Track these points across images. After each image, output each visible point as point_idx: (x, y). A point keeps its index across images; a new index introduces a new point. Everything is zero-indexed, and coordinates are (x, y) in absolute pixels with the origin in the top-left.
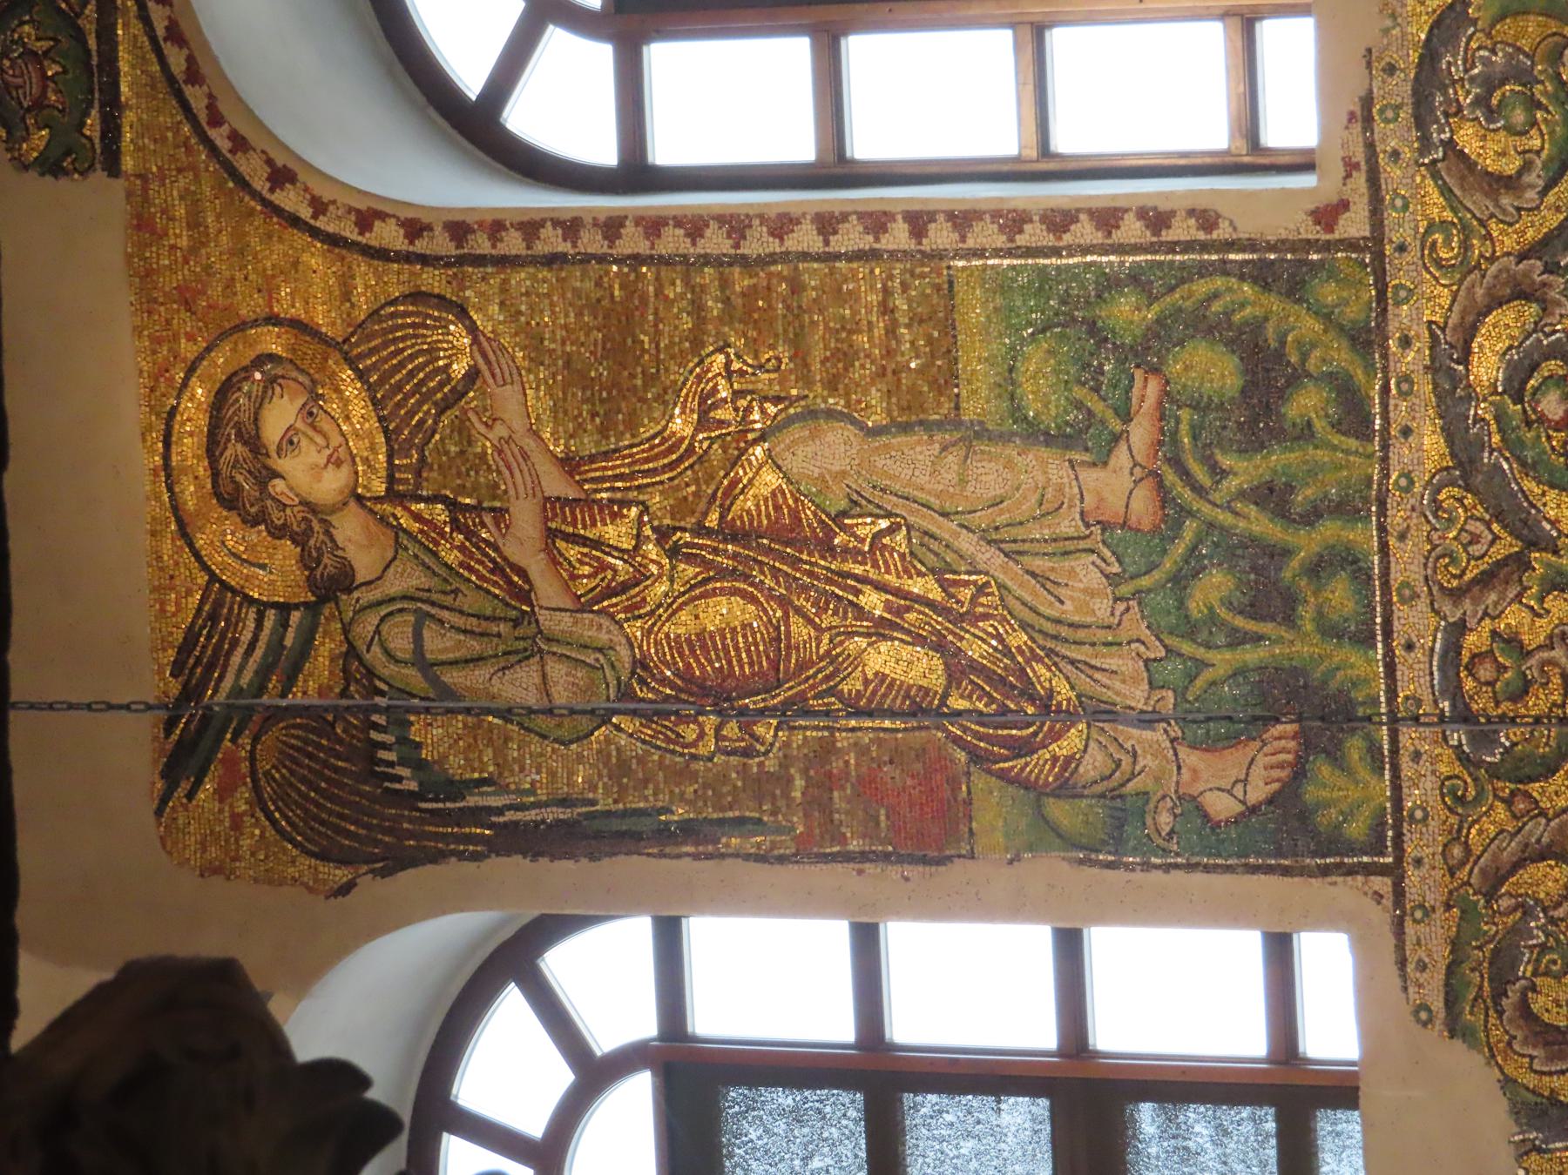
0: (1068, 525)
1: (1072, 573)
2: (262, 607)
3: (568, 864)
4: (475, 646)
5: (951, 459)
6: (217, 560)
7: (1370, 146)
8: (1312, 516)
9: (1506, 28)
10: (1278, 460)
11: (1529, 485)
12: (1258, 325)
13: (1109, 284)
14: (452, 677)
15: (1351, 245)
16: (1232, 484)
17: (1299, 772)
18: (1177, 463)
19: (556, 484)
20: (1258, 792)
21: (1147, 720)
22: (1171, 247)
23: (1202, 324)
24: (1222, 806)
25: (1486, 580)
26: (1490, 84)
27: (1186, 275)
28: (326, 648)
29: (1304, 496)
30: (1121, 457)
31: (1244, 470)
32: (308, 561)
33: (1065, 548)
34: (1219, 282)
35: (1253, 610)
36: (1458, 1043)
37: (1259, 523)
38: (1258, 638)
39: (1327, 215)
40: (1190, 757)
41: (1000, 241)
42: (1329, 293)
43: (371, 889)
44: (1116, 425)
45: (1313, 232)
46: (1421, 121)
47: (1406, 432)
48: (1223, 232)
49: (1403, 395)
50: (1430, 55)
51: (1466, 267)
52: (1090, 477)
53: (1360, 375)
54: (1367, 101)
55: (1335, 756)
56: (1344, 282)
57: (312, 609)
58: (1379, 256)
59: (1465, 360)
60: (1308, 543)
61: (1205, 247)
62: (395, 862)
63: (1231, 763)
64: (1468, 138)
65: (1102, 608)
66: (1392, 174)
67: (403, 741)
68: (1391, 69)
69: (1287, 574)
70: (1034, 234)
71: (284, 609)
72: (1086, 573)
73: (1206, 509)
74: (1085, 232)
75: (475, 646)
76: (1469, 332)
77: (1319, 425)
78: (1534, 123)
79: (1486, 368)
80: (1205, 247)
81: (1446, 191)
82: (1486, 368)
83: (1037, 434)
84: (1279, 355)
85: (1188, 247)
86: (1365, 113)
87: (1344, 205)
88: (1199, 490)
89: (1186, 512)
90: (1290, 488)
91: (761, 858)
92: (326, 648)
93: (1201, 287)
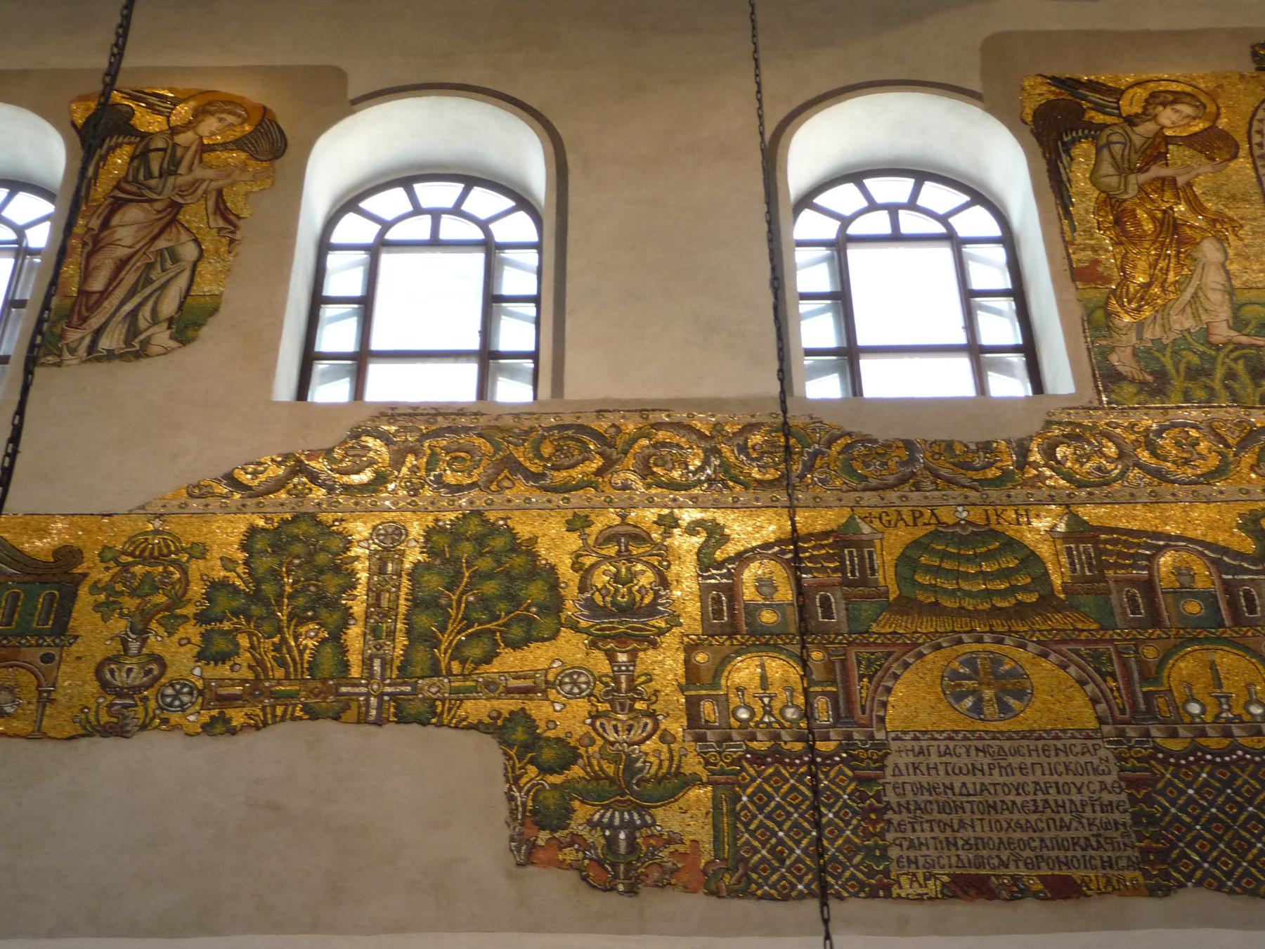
0: (1205, 318)
1: (1187, 319)
2: (1117, 103)
3: (1048, 180)
4: (1118, 158)
5: (1220, 287)
6: (1131, 91)
10: (1245, 377)
14: (1105, 152)
17: (1132, 381)
19: (1181, 181)
20: (1121, 369)
21: (1140, 338)
24: (1114, 358)
25: (1218, 435)
28: (1109, 120)
30: (1233, 333)
31: (1240, 367)
32: (1136, 115)
33: (1196, 316)
35: (1188, 368)
36: (1042, 424)
37: (1220, 372)
38: (1177, 371)
40: (1129, 350)
43: (1026, 131)
52: (1224, 324)
55: (1140, 392)
57: (1120, 116)
60: (1217, 385)
62: (1038, 135)
63: (1130, 361)
65: (1177, 327)
67: (1080, 138)
69: (1204, 379)
71: (1118, 108)
72: (1189, 323)
75: (1118, 158)
83: (1236, 309)
88: (1227, 356)
91: (1062, 233)
92: (1109, 120)
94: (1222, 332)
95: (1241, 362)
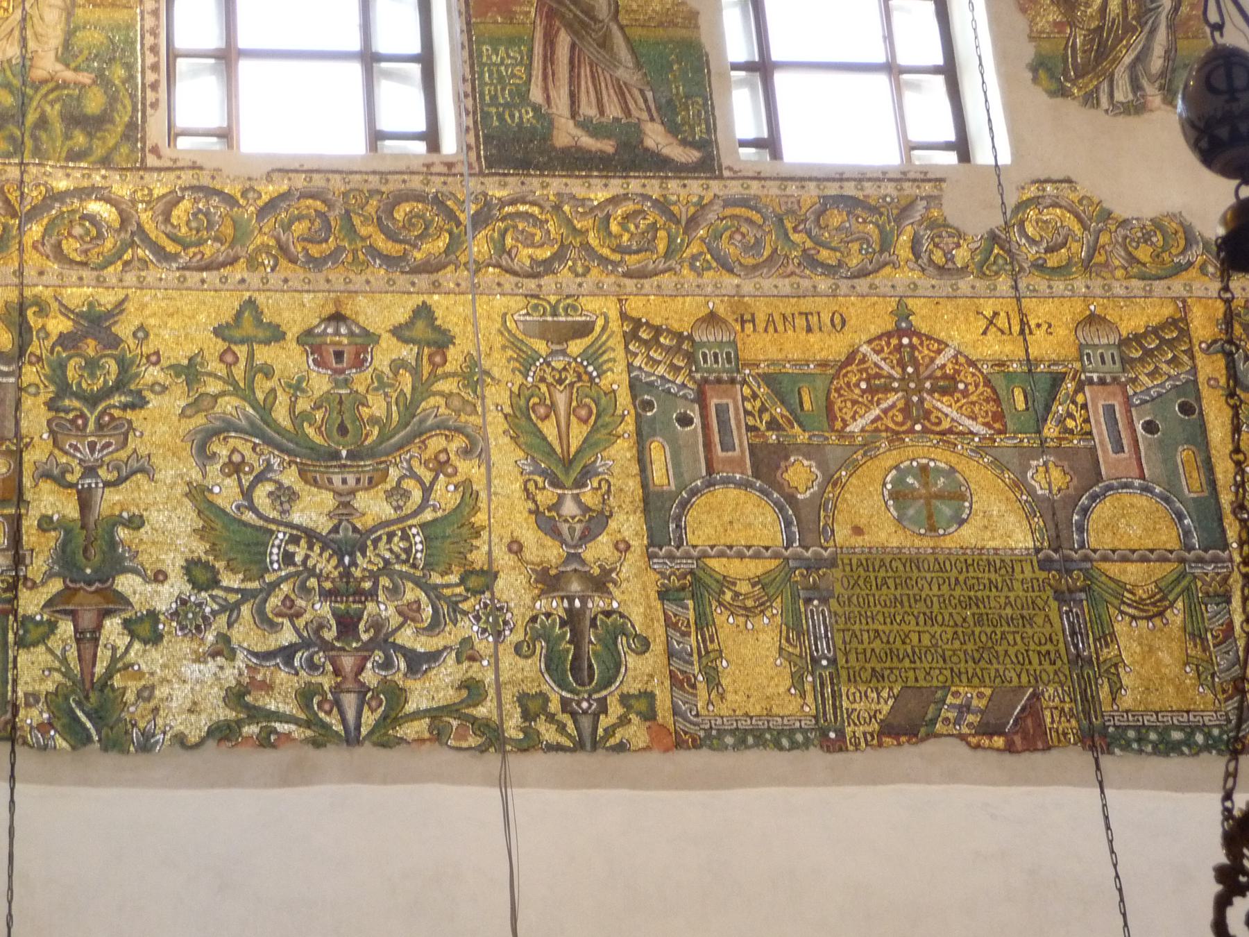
1: (12, 45)
7: (182, 168)
8: (35, 138)
9: (228, 222)
10: (58, 127)
11: (45, 221)
12: (112, 121)
13: (129, 67)
15: (143, 160)
16: (48, 109)
18: (57, 87)
22: (144, 91)
23: (113, 100)
26: (207, 214)
27: (132, 97)
29: (44, 136)
30: (59, 67)
31: (53, 112)
34: (129, 108)
37: (31, 118)
39: (155, 151)
41: (147, 27)
42: (124, 150)
44: (73, 65)
45: (149, 144)
46: (193, 188)
47: (68, 175)
48: (148, 109)
49: (83, 176)
50: (219, 193)
51: (134, 202)
52: (52, 55)
53: (92, 159)
54: (201, 168)
56: (128, 156)
58: (139, 169)
59: (96, 199)
61: (144, 104)
64: (185, 204)
66: (172, 176)
68: (213, 178)
70: (149, 40)
73: (38, 97)
74: (150, 59)
76: (108, 200)
77: (69, 143)
78: (191, 229)
79: (94, 207)
80: (144, 104)
81: (164, 196)
82: (94, 207)
83: (70, 34)
84: (99, 129)
85: (144, 98)
86: (195, 167)
87: (159, 157)
88: (46, 95)
89: (37, 90)
90: (46, 130)
93: (127, 102)
94: (47, 64)
95: (57, 107)
